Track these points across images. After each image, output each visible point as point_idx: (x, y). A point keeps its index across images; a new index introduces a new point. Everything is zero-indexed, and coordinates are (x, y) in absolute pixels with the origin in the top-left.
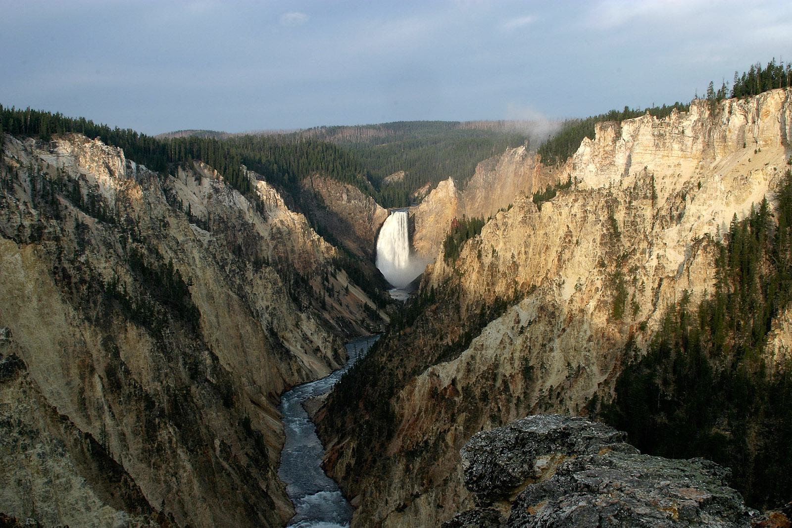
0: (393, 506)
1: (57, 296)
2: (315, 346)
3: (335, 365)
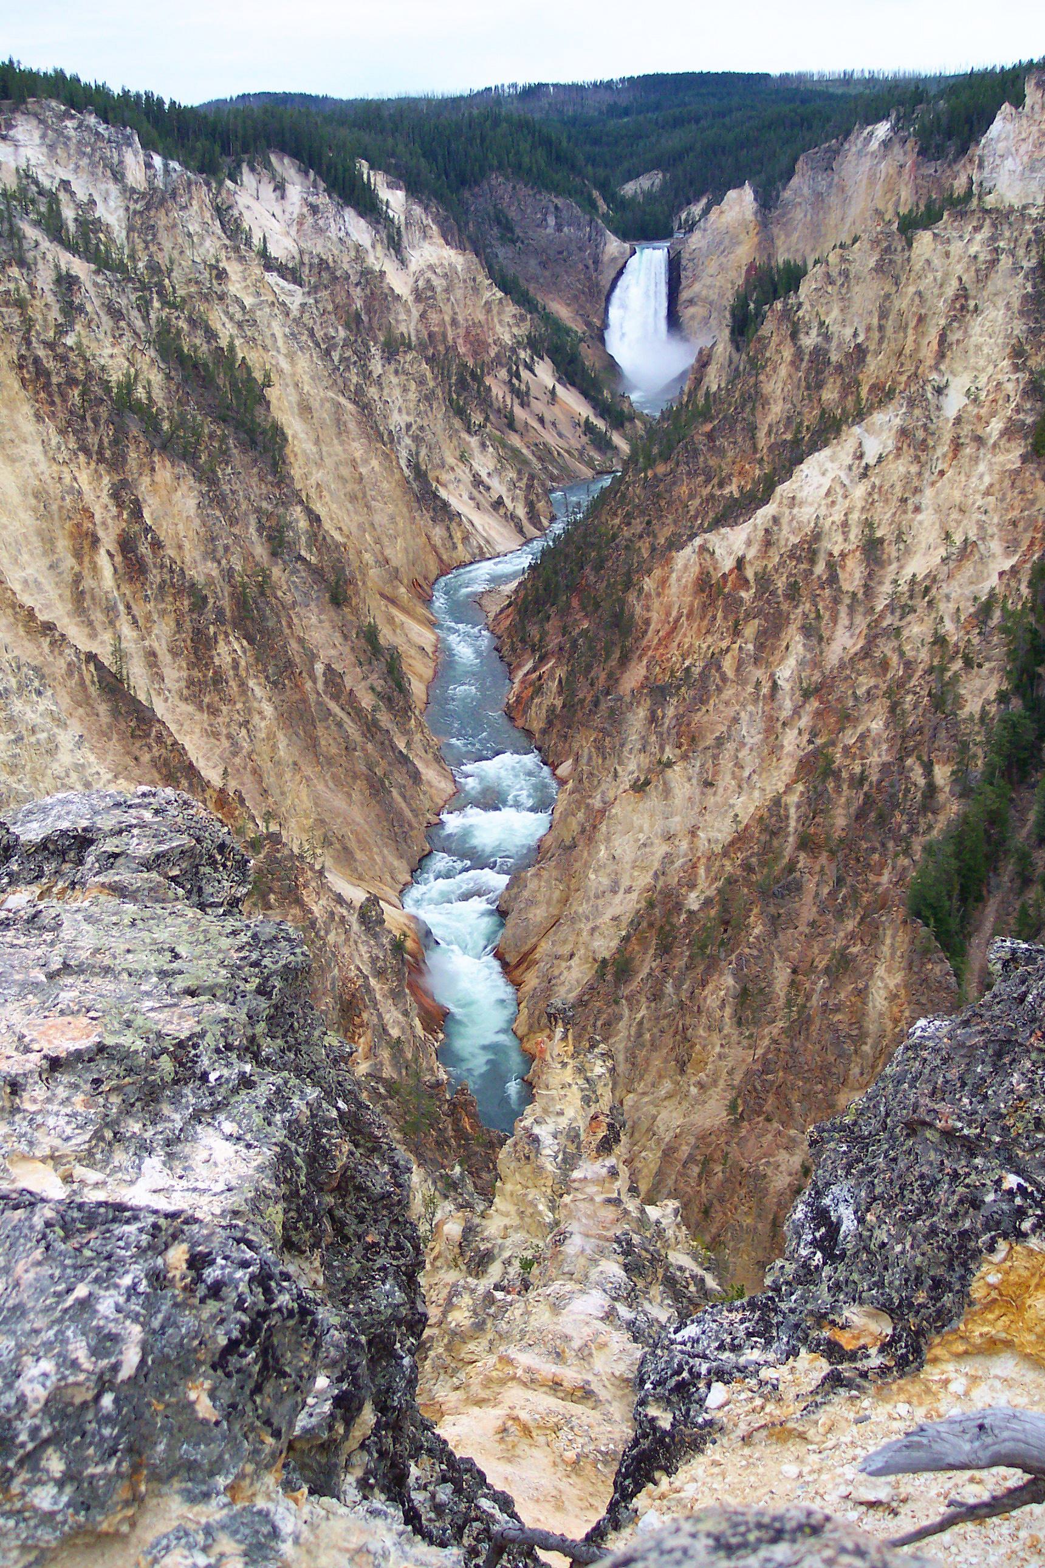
0: (626, 781)
1: (27, 409)
2: (495, 496)
3: (530, 530)
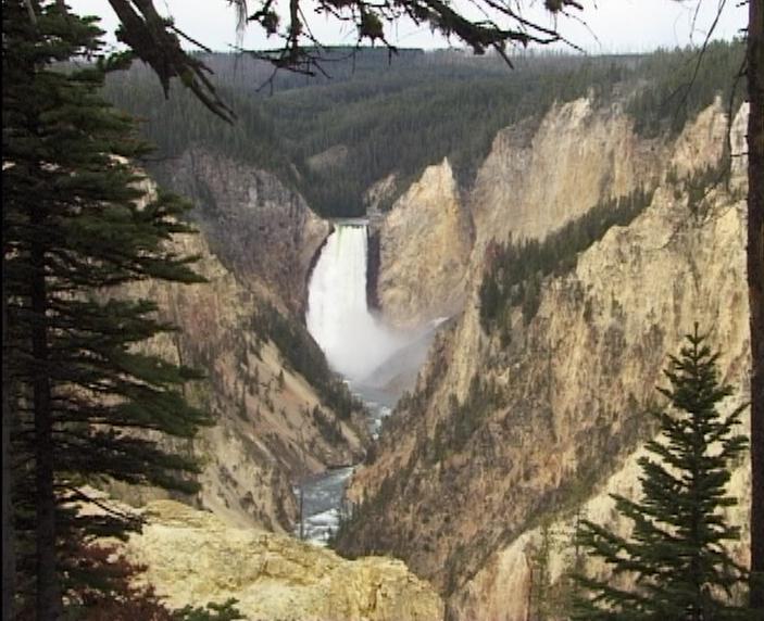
2: (243, 494)
